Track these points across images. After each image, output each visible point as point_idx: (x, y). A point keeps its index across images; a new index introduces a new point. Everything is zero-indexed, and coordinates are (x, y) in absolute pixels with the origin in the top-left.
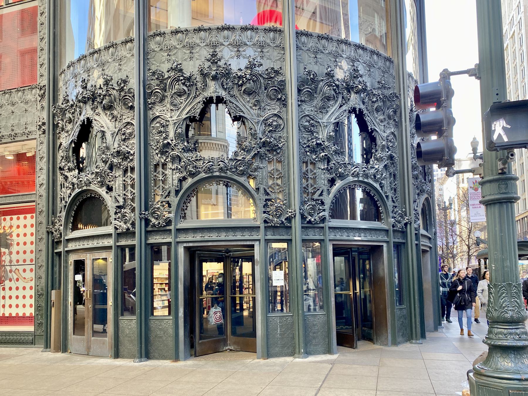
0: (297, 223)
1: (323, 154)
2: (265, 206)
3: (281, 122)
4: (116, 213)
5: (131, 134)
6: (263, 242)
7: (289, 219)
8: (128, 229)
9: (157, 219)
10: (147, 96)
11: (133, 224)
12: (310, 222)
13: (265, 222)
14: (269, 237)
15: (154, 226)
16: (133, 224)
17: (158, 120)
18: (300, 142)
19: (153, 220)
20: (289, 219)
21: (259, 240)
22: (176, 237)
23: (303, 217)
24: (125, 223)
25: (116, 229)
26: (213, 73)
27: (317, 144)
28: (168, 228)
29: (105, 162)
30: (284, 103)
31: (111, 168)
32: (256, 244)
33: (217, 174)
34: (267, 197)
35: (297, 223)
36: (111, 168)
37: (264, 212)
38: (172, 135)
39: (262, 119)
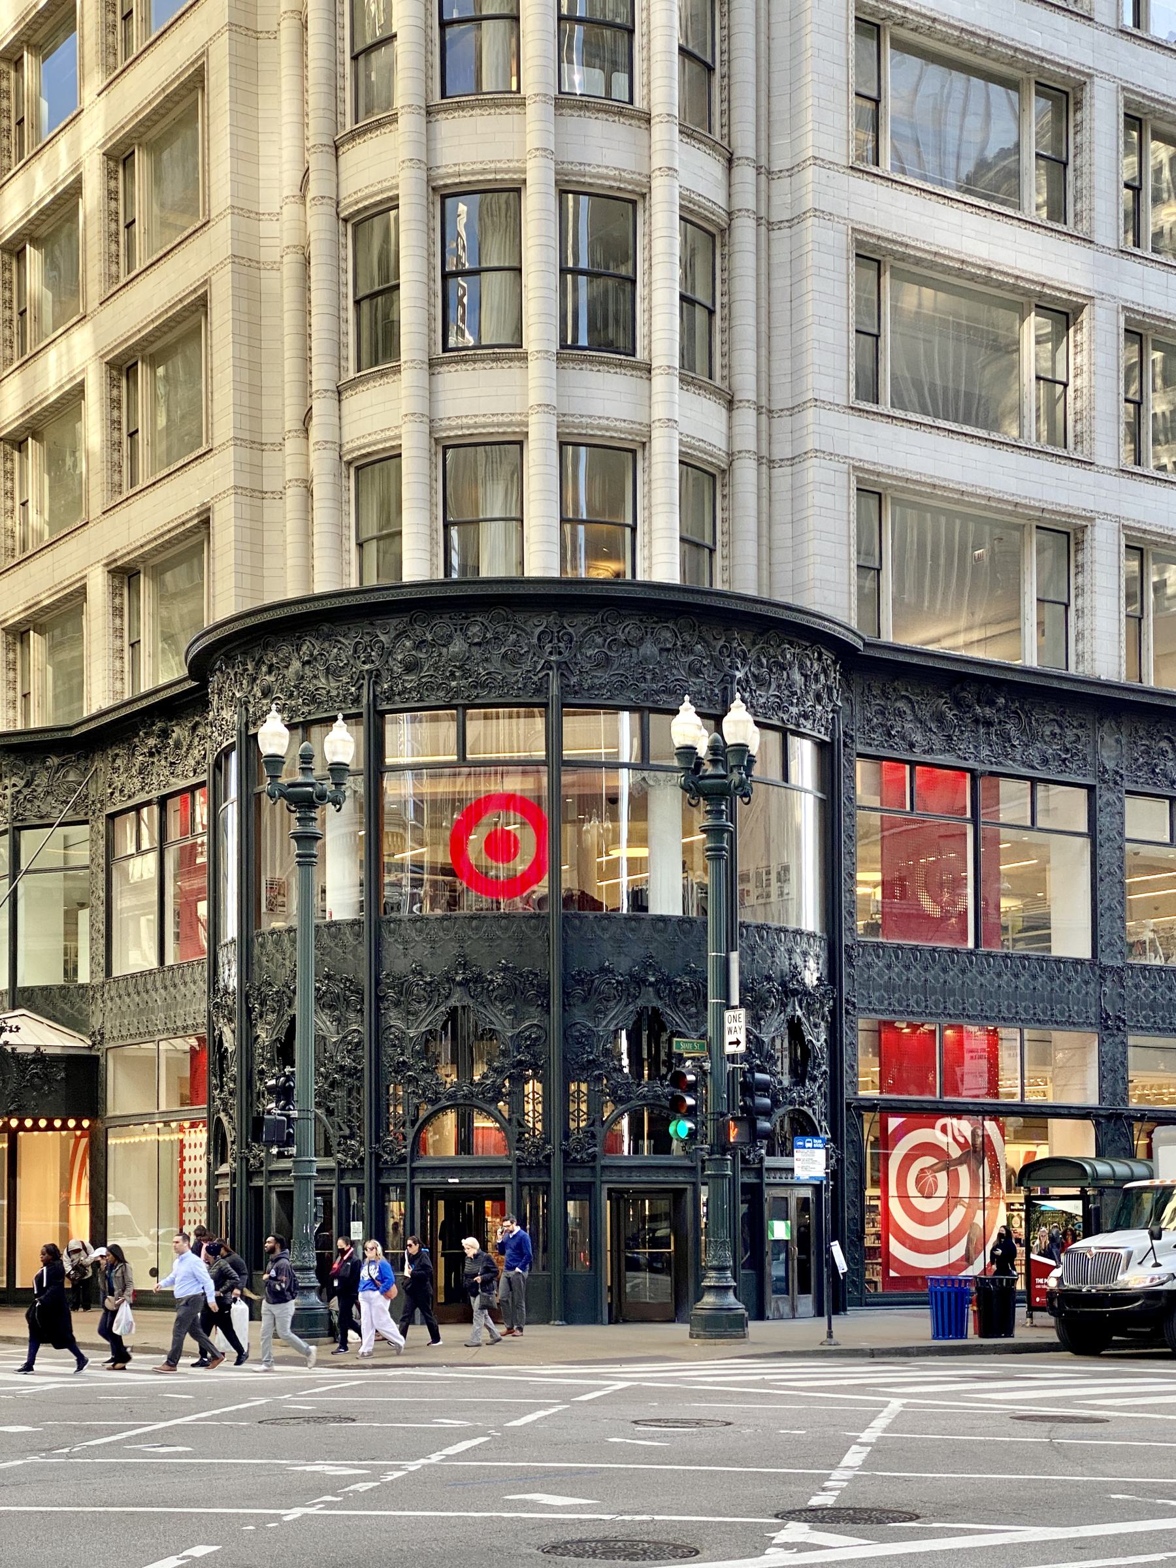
0: (557, 1163)
1: (596, 1073)
2: (519, 1141)
3: (541, 1032)
4: (339, 1144)
5: (358, 1044)
6: (515, 1184)
7: (548, 1158)
8: (355, 1166)
9: (389, 1154)
10: (379, 999)
11: (362, 1160)
12: (575, 1160)
13: (518, 1160)
14: (527, 1180)
15: (386, 1162)
16: (362, 1160)
17: (393, 1030)
18: (565, 1058)
19: (386, 1156)
20: (548, 1158)
21: (511, 1183)
22: (412, 1177)
23: (566, 1154)
24: (352, 1157)
25: (339, 1163)
26: (459, 978)
27: (589, 1061)
28: (403, 1165)
29: (326, 1078)
30: (547, 1009)
31: (333, 1085)
32: (508, 1188)
33: (462, 1101)
34: (521, 1130)
35: (557, 1163)
36: (333, 1085)
37: (518, 1149)
38: (408, 1052)
39: (517, 1031)
